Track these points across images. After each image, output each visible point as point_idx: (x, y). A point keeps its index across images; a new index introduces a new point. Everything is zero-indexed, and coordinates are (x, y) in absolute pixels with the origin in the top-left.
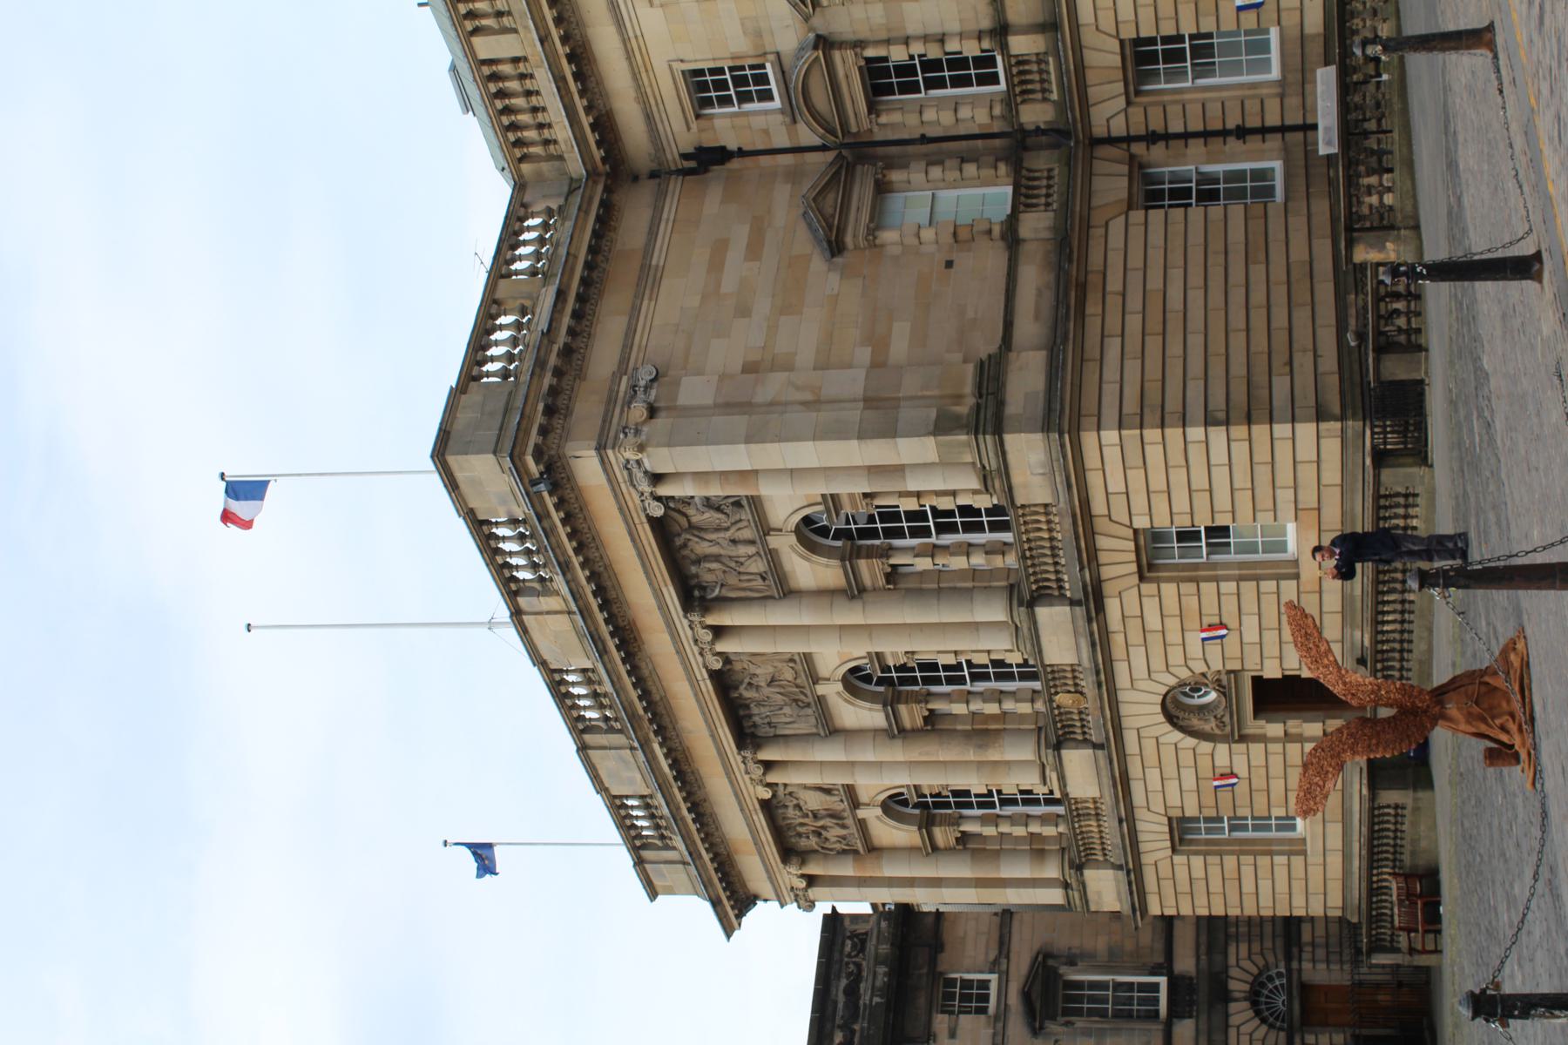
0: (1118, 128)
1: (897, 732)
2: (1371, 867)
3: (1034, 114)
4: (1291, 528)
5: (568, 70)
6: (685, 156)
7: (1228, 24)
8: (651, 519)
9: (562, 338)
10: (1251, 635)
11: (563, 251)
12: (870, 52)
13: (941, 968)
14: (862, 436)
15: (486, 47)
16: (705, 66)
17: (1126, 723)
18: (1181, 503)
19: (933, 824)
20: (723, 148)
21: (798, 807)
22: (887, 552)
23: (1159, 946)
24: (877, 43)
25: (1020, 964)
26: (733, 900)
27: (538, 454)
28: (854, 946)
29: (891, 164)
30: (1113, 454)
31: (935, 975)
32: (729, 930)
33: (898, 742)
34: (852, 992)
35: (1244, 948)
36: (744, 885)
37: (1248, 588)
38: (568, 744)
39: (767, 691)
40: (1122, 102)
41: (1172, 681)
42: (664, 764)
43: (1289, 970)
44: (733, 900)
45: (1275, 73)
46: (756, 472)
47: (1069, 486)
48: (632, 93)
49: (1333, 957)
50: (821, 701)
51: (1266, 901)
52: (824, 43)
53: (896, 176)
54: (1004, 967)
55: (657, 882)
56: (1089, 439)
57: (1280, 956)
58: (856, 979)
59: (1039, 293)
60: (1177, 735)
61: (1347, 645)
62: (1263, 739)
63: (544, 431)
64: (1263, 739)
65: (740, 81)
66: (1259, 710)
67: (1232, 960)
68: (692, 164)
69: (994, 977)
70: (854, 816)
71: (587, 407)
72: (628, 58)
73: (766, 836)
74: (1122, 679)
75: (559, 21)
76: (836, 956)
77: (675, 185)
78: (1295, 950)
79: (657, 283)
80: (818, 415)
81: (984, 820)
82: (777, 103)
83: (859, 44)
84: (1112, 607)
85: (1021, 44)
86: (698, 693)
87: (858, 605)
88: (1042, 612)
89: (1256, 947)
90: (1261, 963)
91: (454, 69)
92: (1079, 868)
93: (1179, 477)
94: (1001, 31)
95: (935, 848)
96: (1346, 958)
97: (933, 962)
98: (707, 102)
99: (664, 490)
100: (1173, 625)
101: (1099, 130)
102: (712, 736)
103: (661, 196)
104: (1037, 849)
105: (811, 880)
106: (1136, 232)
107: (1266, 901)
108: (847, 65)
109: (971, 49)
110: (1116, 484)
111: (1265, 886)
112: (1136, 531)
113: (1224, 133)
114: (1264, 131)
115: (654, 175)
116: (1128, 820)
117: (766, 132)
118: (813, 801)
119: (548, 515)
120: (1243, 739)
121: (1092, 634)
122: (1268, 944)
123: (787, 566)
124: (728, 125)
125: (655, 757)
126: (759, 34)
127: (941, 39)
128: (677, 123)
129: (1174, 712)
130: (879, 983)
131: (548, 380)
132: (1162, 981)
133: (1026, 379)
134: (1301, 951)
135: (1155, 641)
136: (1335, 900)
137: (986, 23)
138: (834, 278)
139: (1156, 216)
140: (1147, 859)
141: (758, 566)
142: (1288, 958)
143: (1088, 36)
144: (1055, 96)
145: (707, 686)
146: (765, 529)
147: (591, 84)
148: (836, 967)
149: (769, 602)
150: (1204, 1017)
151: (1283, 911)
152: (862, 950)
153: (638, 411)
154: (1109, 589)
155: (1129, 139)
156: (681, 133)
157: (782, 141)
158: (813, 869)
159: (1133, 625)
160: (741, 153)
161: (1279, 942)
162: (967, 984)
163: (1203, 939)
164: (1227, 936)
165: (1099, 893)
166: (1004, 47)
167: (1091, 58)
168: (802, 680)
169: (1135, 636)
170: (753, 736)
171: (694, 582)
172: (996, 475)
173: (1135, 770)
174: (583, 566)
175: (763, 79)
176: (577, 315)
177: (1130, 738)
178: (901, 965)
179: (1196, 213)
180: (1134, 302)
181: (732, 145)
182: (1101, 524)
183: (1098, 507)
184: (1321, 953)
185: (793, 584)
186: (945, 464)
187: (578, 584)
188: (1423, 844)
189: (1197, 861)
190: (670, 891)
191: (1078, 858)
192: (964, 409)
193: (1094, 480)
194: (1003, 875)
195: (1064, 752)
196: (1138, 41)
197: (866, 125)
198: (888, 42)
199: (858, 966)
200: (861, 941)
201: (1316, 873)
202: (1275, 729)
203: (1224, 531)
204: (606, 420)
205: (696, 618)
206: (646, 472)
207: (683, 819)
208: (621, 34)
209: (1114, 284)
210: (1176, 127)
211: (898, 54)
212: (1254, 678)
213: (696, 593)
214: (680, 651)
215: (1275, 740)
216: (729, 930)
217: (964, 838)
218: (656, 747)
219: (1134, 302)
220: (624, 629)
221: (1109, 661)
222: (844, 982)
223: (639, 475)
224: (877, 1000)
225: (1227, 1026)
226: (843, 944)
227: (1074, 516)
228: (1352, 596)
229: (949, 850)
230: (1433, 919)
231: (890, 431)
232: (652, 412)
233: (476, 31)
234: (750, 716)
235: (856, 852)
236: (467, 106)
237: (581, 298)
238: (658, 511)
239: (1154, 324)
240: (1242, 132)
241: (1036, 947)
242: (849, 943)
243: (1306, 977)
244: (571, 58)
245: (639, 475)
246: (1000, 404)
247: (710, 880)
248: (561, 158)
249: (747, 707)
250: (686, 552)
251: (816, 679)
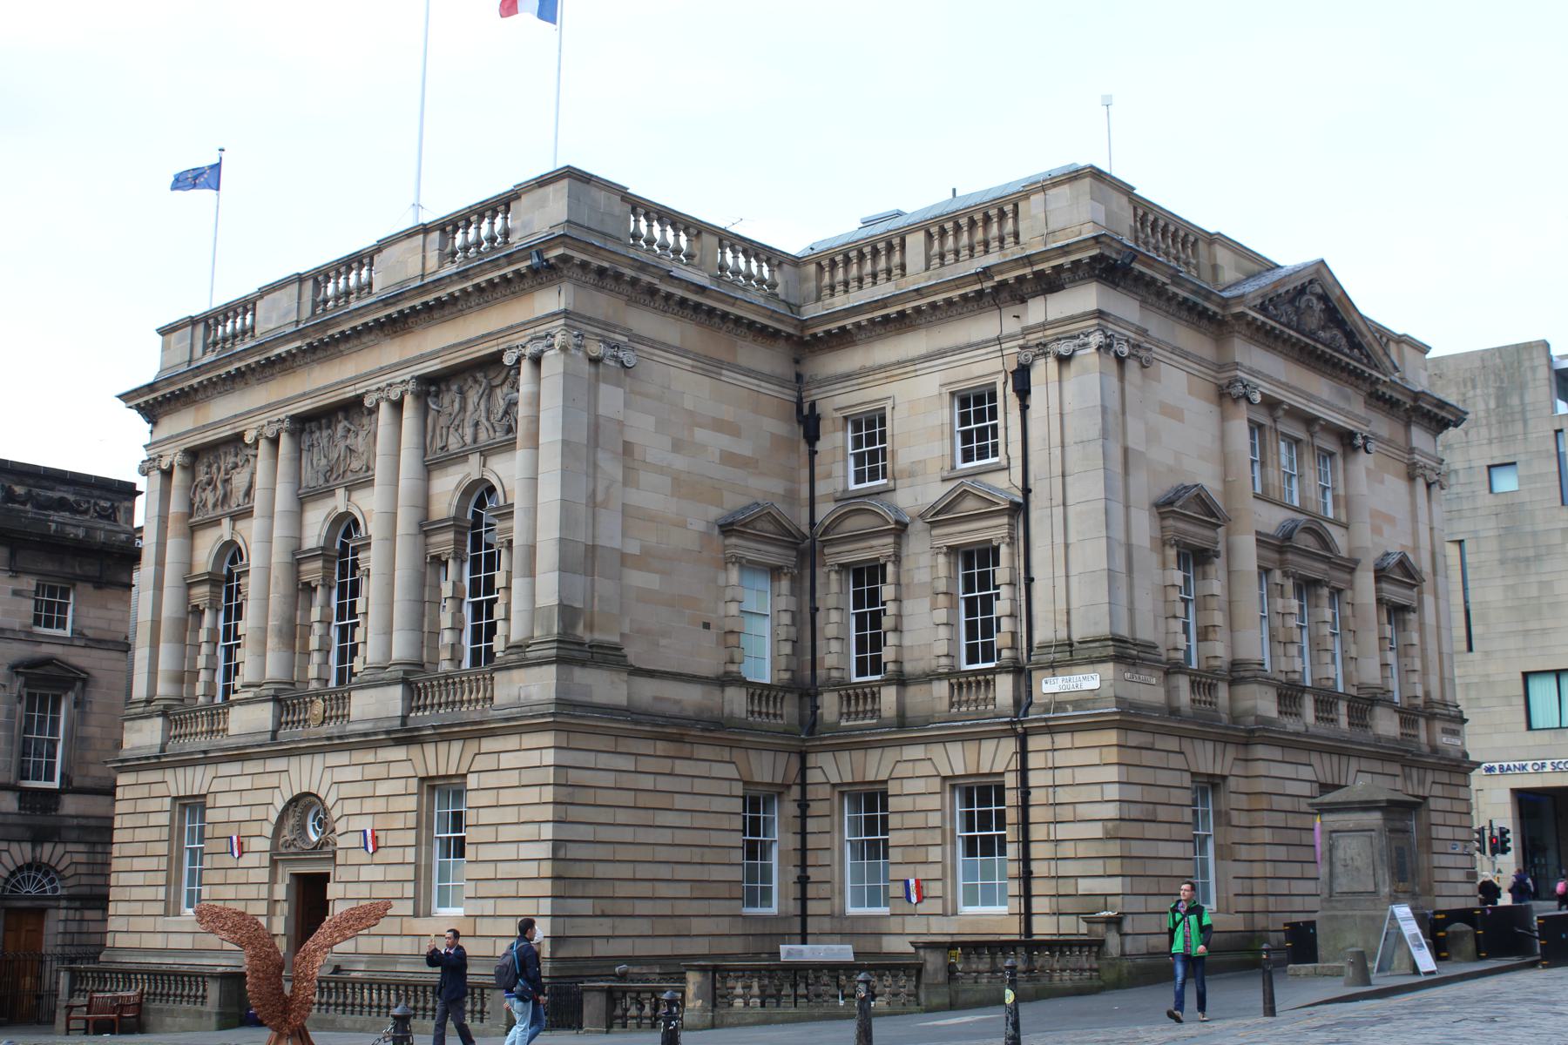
0: (814, 776)
1: (298, 558)
2: (149, 973)
3: (829, 705)
4: (460, 911)
5: (892, 310)
6: (813, 405)
7: (895, 872)
8: (501, 353)
9: (665, 288)
10: (367, 873)
11: (739, 294)
12: (890, 568)
13: (79, 586)
14: (563, 541)
15: (916, 242)
16: (888, 428)
17: (294, 761)
18: (487, 816)
19: (212, 585)
20: (818, 438)
21: (235, 466)
22: (459, 557)
23: (88, 783)
24: (898, 575)
25: (79, 658)
26: (153, 403)
27: (564, 259)
28: (104, 509)
29: (795, 581)
30: (533, 758)
31: (73, 580)
32: (125, 397)
33: (289, 559)
34: (62, 505)
35: (82, 858)
36: (167, 414)
37: (409, 872)
38: (306, 265)
39: (342, 445)
40: (835, 780)
41: (329, 803)
42: (281, 350)
43: (59, 898)
44: (153, 403)
45: (851, 911)
46: (537, 448)
47: (507, 720)
48: (869, 364)
49: (68, 937)
50: (330, 492)
51: (124, 879)
52: (900, 530)
53: (785, 585)
54: (77, 642)
55: (174, 336)
56: (548, 739)
57: (72, 891)
58: (73, 509)
59: (677, 702)
60: (280, 805)
61: (353, 958)
62: (273, 881)
63: (584, 265)
64: (273, 881)
65: (873, 456)
66: (297, 877)
67: (70, 847)
68: (806, 411)
69: (68, 633)
70: (224, 516)
71: (602, 304)
72: (899, 363)
73: (211, 436)
75: (933, 306)
76: (96, 493)
77: (789, 395)
78: (77, 904)
79: (706, 373)
80: (583, 505)
81: (213, 631)
82: (853, 486)
83: (898, 560)
84: (399, 753)
85: (889, 696)
86: (343, 384)
87: (413, 529)
88: (397, 691)
89: (82, 869)
90: (67, 873)
91: (899, 214)
92: (164, 714)
93: (510, 815)
94: (901, 680)
95: (190, 586)
96: (67, 949)
97: (86, 579)
98: (857, 427)
99: (525, 366)
100: (380, 805)
101: (812, 760)
102: (304, 394)
103: (781, 382)
104: (184, 677)
105: (167, 474)
106: (724, 788)
107: (124, 879)
108: (881, 548)
109: (887, 654)
110: (507, 761)
111: (139, 879)
112: (465, 776)
113: (803, 866)
114: (803, 899)
115: (799, 377)
116: (206, 759)
117: (829, 476)
118: (240, 480)
119: (510, 264)
120: (274, 863)
121: (375, 734)
122: (84, 880)
123: (452, 470)
124: (837, 443)
125: (288, 342)
126: (912, 475)
127: (897, 629)
128: (842, 400)
129: (302, 803)
130: (69, 529)
131: (629, 272)
132: (56, 784)
133: (604, 687)
134: (76, 909)
135: (367, 789)
136: (122, 941)
137: (908, 668)
138: (700, 526)
139: (737, 805)
141: (454, 444)
142: (70, 898)
143: (891, 754)
144: (844, 723)
145: (350, 392)
146: (486, 452)
147: (879, 330)
148: (86, 491)
149: (421, 452)
150: (19, 820)
151: (114, 894)
152: (101, 516)
153: (596, 349)
154: (415, 751)
155: (803, 785)
156: (834, 403)
157: (821, 488)
158: (178, 477)
159: (380, 771)
160: (813, 453)
161: (86, 890)
162: (63, 608)
163: (93, 822)
164: (94, 843)
165: (140, 730)
166: (887, 682)
167: (874, 755)
168: (350, 477)
169: (371, 772)
170: (302, 431)
171: (443, 387)
172: (521, 658)
173: (251, 767)
174: (464, 291)
175: (874, 477)
176: (683, 302)
177: (280, 764)
178: (83, 550)
179: (738, 839)
180: (664, 783)
181: (819, 446)
182: (472, 746)
183: (488, 744)
184: (73, 927)
185: (435, 474)
186: (533, 612)
187: (448, 285)
188: (168, 1020)
189: (164, 819)
190: (165, 347)
191: (174, 713)
192: (580, 631)
193: (512, 742)
194: (162, 645)
195: (270, 705)
196: (885, 796)
197: (830, 561)
198: (898, 584)
199: (86, 512)
200: (109, 515)
201: (147, 924)
202: (281, 892)
203: (460, 853)
204: (590, 320)
205: (411, 386)
206: (542, 351)
207: (231, 363)
208: (919, 358)
209: (681, 767)
210: (811, 825)
211: (887, 592)
213: (433, 389)
214: (382, 371)
215: (271, 892)
216: (125, 397)
217: (197, 612)
218: (298, 344)
219: (664, 783)
220: (405, 323)
221: (350, 748)
222: (71, 498)
223: (541, 345)
224: (53, 526)
225: (9, 841)
226: (107, 499)
227: (481, 723)
228: (396, 963)
229: (188, 598)
230: (100, 1027)
231: (564, 567)
232: (595, 361)
233: (929, 235)
234: (320, 429)
235: (191, 515)
236: (867, 223)
237: (697, 307)
238: (508, 359)
239: (644, 800)
240: (803, 881)
241: (93, 672)
242: (108, 504)
243: (51, 912)
244: (902, 314)
245: (541, 345)
246: (583, 664)
247: (173, 384)
248: (818, 299)
249: (329, 427)
250: (470, 382)
251: (350, 489)
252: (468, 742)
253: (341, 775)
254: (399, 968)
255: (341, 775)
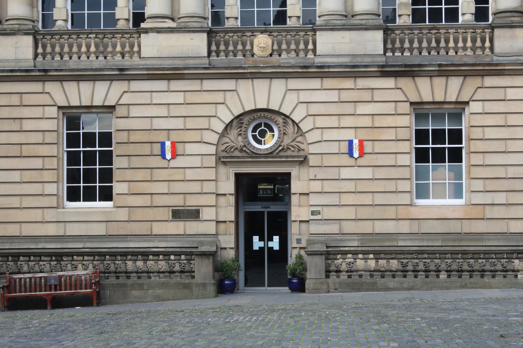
10: (345, 173)
60: (228, 118)
61: (339, 237)
74: (294, 83)
84: (389, 82)
88: (379, 35)
111: (16, 176)
112: (467, 103)
116: (122, 74)
135: (348, 108)
140: (52, 87)
154: (405, 83)
159: (366, 96)
169: (346, 96)
173: (176, 85)
182: (474, 82)
183: (489, 81)
191: (41, 32)
201: (37, 215)
212: (289, 175)
228: (397, 240)
252: (469, 80)
253: (304, 96)
254: (401, 243)
255: (304, 96)
